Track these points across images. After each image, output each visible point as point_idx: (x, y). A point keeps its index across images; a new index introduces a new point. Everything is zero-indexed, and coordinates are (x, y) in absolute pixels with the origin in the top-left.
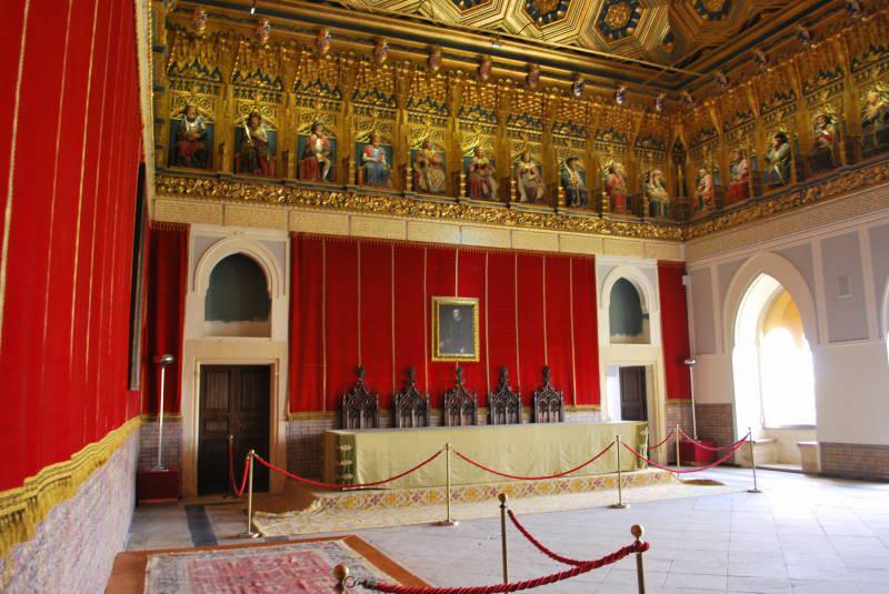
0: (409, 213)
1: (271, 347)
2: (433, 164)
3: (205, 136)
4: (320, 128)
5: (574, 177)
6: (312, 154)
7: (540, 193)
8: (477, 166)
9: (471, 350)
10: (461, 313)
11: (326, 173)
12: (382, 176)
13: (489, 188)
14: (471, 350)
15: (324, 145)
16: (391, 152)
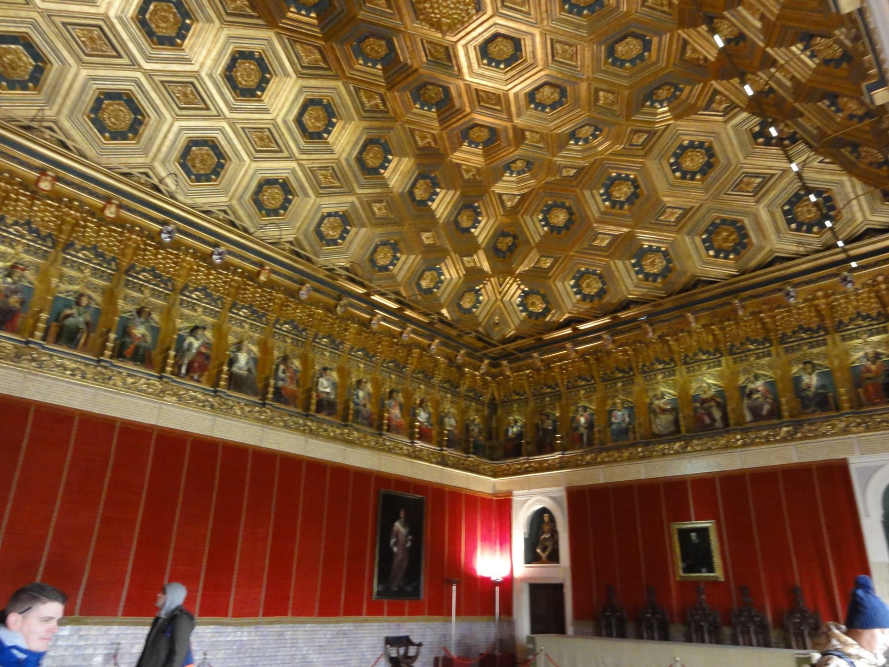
0: (643, 458)
1: (560, 571)
2: (664, 411)
3: (520, 435)
4: (580, 409)
5: (812, 380)
6: (576, 429)
7: (767, 408)
8: (704, 401)
9: (711, 570)
10: (698, 536)
11: (585, 439)
12: (623, 432)
13: (713, 420)
14: (711, 570)
15: (586, 420)
16: (631, 410)
